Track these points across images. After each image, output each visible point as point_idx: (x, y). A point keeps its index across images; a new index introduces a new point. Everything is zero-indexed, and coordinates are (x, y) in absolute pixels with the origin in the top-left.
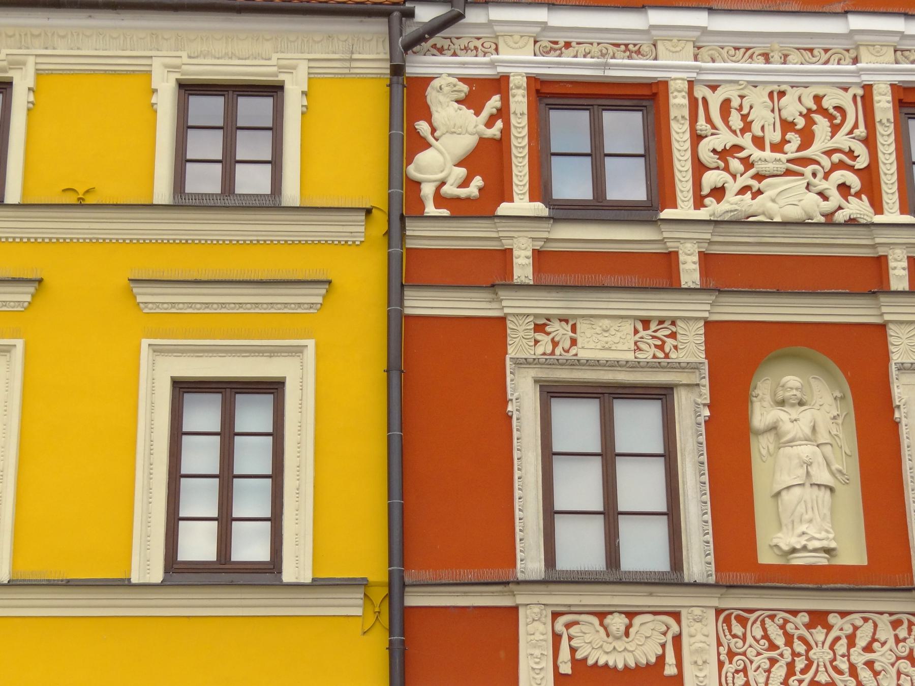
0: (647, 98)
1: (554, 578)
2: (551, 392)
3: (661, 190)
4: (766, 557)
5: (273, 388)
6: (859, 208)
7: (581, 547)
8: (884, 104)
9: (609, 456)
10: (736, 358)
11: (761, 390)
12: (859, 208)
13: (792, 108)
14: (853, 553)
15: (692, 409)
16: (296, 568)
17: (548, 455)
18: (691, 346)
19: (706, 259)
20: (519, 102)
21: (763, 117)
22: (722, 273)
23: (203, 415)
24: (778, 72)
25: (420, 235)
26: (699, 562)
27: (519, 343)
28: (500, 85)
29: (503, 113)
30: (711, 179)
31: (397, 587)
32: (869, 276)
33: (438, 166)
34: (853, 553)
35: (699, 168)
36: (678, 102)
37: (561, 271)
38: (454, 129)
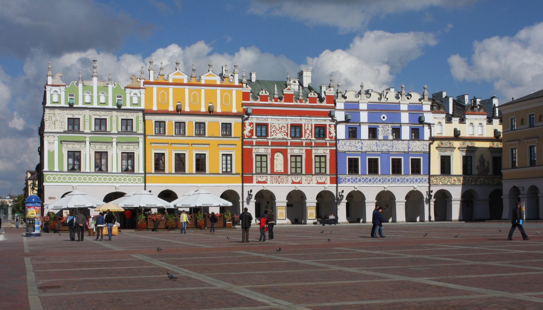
0: (266, 125)
1: (257, 174)
2: (256, 155)
3: (267, 135)
4: (275, 171)
5: (231, 155)
6: (286, 137)
7: (259, 170)
8: (289, 126)
9: (261, 161)
10: (274, 152)
11: (276, 155)
12: (286, 137)
13: (280, 126)
14: (283, 171)
15: (269, 157)
16: (234, 172)
17: (256, 161)
18: (269, 151)
19: (271, 142)
20: (254, 125)
21: (278, 127)
22: (273, 144)
23: (224, 158)
24: (279, 122)
25: (245, 140)
26: (269, 172)
27: (254, 151)
28: (252, 123)
29: (253, 127)
30: (272, 134)
31: (242, 174)
32: (286, 144)
33: (246, 132)
34: (283, 171)
35: (271, 132)
36: (269, 126)
37: (259, 144)
38: (248, 128)
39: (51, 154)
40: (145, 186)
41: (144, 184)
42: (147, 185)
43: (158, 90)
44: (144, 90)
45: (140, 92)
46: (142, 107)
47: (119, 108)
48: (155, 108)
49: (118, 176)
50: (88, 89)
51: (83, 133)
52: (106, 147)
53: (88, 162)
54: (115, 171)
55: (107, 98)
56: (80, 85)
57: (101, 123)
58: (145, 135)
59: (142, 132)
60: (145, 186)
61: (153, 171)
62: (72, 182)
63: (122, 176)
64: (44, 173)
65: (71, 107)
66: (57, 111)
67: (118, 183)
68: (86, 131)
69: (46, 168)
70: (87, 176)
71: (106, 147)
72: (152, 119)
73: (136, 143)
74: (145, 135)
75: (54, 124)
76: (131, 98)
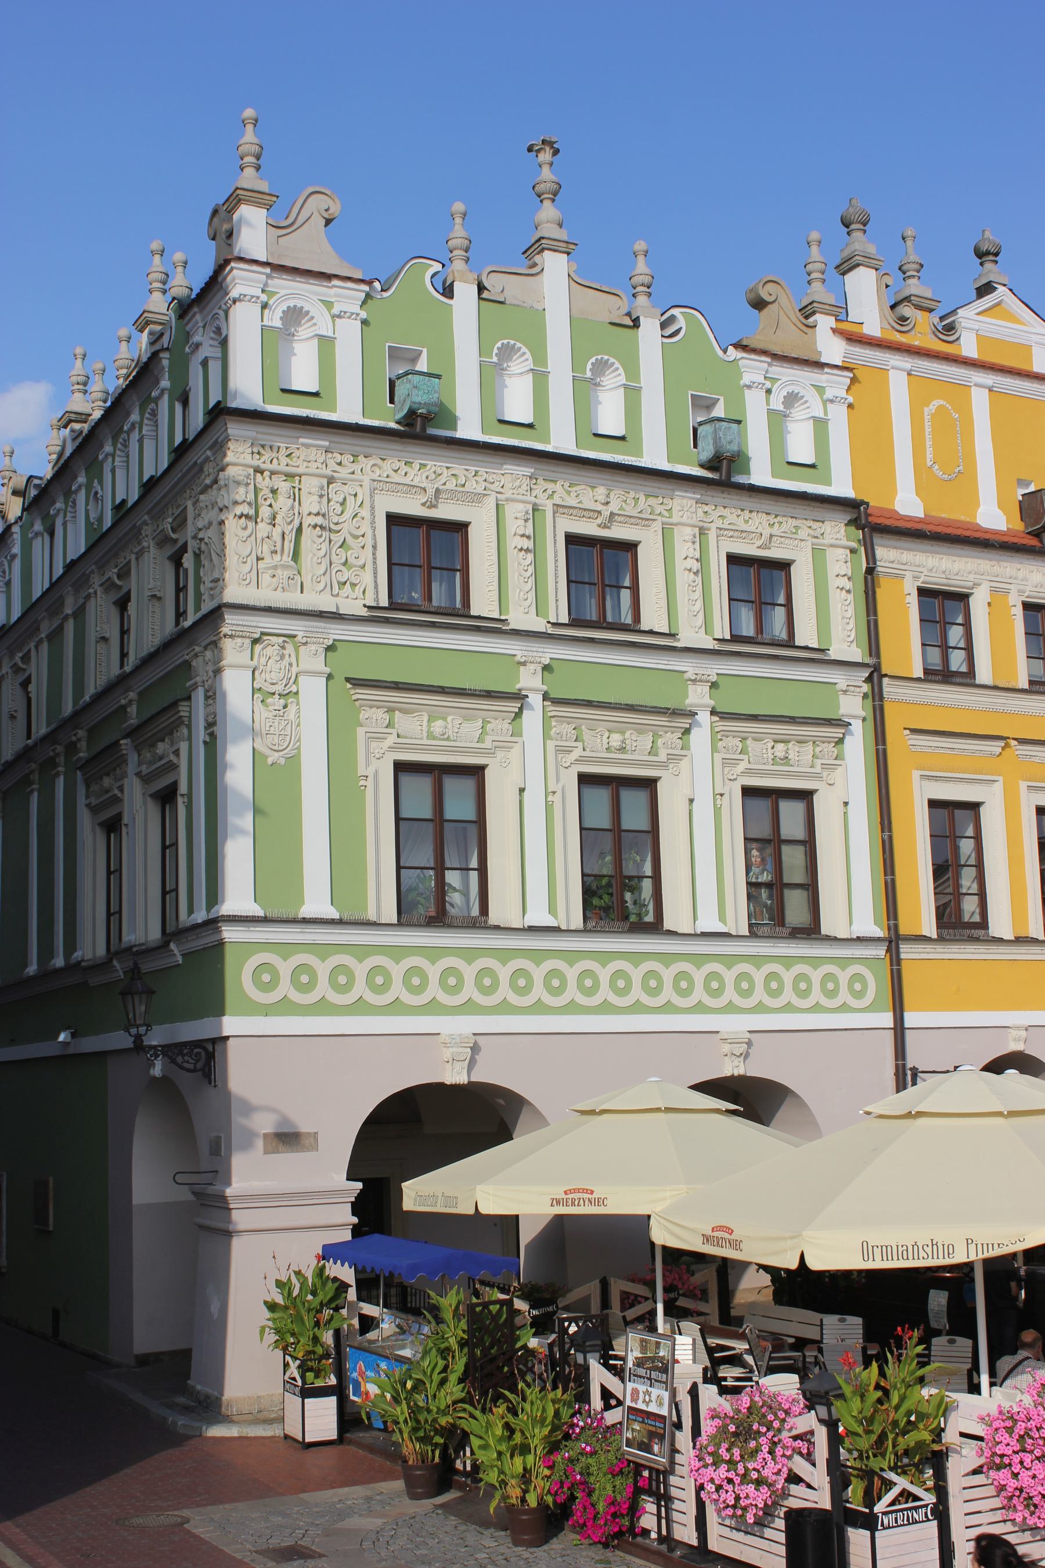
39: (279, 777)
40: (899, 1030)
41: (887, 1019)
42: (911, 1019)
43: (921, 391)
44: (845, 378)
45: (820, 389)
46: (842, 487)
47: (723, 474)
48: (908, 503)
49: (730, 960)
50: (510, 328)
51: (494, 628)
52: (646, 741)
53: (534, 861)
54: (709, 922)
55: (632, 394)
56: (465, 292)
57: (600, 567)
58: (875, 676)
59: (857, 654)
60: (899, 1030)
61: (929, 926)
62: (433, 1008)
63: (757, 960)
64: (230, 934)
65: (421, 428)
66: (309, 454)
67: (730, 1008)
68: (520, 617)
69: (238, 896)
70: (538, 956)
71: (646, 741)
72: (910, 567)
73: (829, 722)
74: (875, 676)
75: (296, 556)
76: (777, 421)
